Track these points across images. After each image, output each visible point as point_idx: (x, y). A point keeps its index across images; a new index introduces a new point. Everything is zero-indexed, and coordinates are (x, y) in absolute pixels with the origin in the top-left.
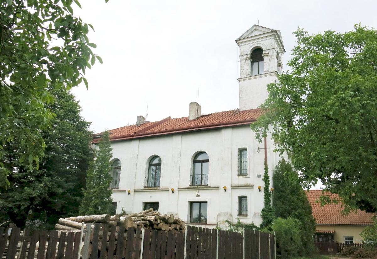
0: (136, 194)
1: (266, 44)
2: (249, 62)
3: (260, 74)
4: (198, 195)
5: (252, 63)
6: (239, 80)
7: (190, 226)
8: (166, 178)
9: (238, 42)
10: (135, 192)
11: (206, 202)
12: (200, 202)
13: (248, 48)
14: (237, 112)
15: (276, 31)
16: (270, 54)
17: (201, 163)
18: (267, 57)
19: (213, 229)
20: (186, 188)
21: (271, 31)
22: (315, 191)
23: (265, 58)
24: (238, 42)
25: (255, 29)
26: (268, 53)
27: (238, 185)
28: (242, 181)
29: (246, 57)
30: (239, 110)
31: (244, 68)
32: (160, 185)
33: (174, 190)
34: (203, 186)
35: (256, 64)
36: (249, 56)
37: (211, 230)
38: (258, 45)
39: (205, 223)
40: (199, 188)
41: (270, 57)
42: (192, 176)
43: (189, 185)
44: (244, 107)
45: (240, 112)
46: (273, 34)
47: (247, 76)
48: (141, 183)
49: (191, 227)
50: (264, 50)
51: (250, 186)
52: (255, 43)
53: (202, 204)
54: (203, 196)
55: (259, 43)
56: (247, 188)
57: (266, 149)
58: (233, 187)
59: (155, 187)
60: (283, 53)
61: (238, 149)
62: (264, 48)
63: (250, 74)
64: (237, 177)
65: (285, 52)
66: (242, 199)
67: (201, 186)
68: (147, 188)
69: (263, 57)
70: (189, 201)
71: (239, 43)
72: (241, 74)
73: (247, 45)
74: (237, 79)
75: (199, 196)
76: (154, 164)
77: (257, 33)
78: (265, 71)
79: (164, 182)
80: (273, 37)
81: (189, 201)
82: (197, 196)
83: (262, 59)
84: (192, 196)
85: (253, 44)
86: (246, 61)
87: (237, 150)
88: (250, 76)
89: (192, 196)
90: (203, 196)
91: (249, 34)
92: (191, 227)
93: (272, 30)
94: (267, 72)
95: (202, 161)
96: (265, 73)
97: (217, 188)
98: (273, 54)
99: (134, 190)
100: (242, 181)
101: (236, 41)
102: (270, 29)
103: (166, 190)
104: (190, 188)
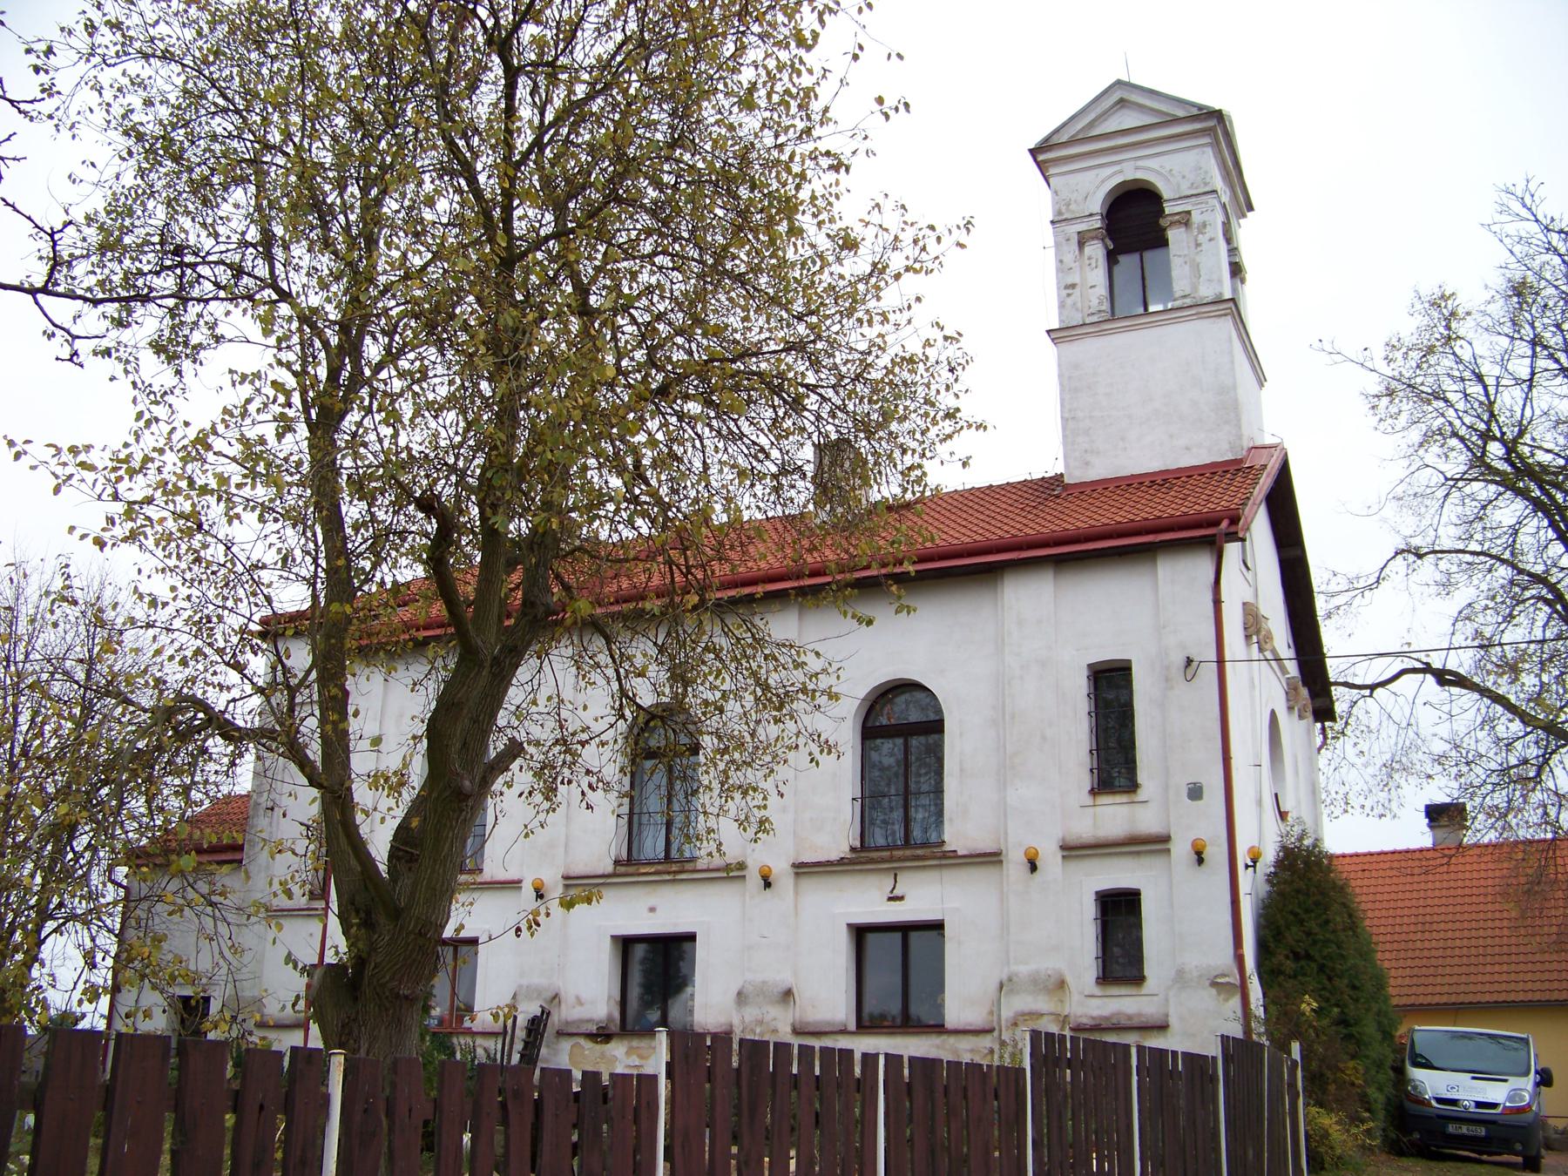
0: (808, 884)
1: (1175, 171)
2: (1096, 251)
3: (1118, 314)
4: (897, 892)
5: (1112, 258)
6: (1054, 335)
7: (1127, 1047)
8: (973, 796)
9: (1041, 158)
10: (797, 874)
11: (937, 926)
12: (905, 929)
13: (1093, 187)
14: (1049, 489)
15: (1218, 115)
16: (1196, 218)
17: (900, 741)
18: (1183, 229)
19: (911, 1059)
20: (829, 863)
21: (1195, 111)
22: (1357, 855)
23: (1172, 234)
24: (1041, 158)
25: (1122, 101)
26: (1189, 212)
27: (1092, 841)
28: (1114, 817)
29: (1083, 227)
30: (1058, 478)
31: (1077, 280)
32: (946, 838)
33: (774, 871)
34: (875, 855)
35: (1128, 262)
36: (1097, 223)
37: (1174, 1053)
38: (1139, 175)
39: (939, 1028)
40: (899, 860)
41: (1200, 232)
42: (858, 805)
43: (847, 849)
44: (1087, 464)
45: (1067, 487)
46: (1197, 126)
47: (1095, 319)
48: (836, 833)
49: (906, 1060)
50: (1165, 196)
51: (1156, 844)
52: (1124, 164)
53: (914, 936)
54: (922, 896)
55: (1140, 163)
56: (1138, 853)
57: (1221, 661)
58: (1073, 850)
59: (907, 843)
60: (1244, 216)
61: (1089, 666)
62: (1166, 193)
63: (1106, 306)
64: (1089, 800)
65: (1250, 208)
66: (1119, 910)
67: (908, 853)
68: (865, 857)
69: (1164, 230)
70: (849, 926)
71: (1045, 162)
72: (1062, 305)
73: (1091, 174)
74: (1048, 332)
75: (901, 898)
76: (902, 730)
77: (1129, 119)
78: (1177, 295)
79: (965, 818)
80: (1207, 140)
81: (849, 926)
82: (890, 899)
83: (1164, 243)
84: (869, 901)
85: (1117, 168)
86: (1088, 250)
87: (1085, 673)
88: (1108, 316)
89: (869, 901)
90: (922, 896)
91: (1091, 125)
92: (906, 1060)
93: (1200, 107)
94: (1188, 301)
95: (906, 731)
96: (1178, 303)
97: (992, 858)
98: (1209, 215)
99: (794, 866)
100: (1114, 817)
101: (1034, 152)
102: (1193, 105)
103: (733, 872)
104: (851, 862)
